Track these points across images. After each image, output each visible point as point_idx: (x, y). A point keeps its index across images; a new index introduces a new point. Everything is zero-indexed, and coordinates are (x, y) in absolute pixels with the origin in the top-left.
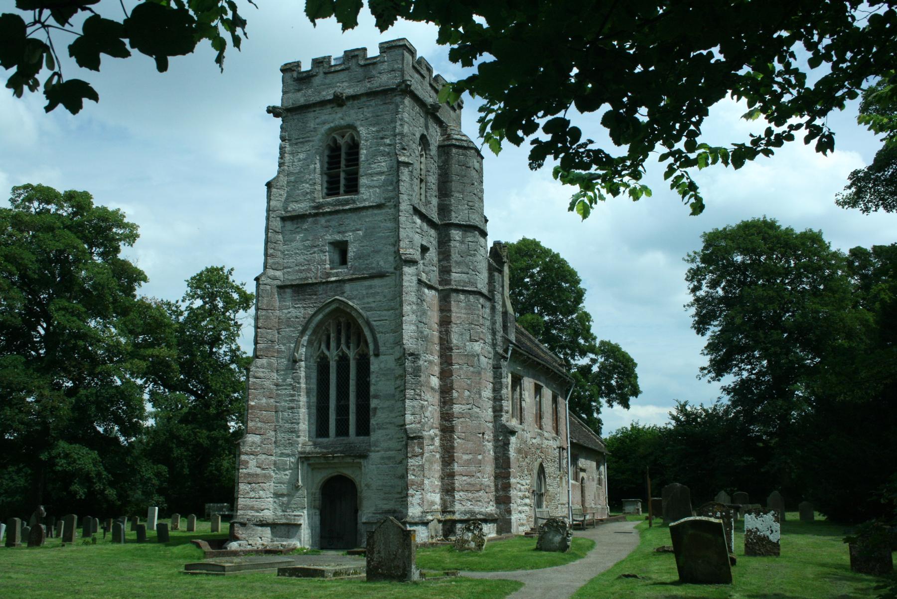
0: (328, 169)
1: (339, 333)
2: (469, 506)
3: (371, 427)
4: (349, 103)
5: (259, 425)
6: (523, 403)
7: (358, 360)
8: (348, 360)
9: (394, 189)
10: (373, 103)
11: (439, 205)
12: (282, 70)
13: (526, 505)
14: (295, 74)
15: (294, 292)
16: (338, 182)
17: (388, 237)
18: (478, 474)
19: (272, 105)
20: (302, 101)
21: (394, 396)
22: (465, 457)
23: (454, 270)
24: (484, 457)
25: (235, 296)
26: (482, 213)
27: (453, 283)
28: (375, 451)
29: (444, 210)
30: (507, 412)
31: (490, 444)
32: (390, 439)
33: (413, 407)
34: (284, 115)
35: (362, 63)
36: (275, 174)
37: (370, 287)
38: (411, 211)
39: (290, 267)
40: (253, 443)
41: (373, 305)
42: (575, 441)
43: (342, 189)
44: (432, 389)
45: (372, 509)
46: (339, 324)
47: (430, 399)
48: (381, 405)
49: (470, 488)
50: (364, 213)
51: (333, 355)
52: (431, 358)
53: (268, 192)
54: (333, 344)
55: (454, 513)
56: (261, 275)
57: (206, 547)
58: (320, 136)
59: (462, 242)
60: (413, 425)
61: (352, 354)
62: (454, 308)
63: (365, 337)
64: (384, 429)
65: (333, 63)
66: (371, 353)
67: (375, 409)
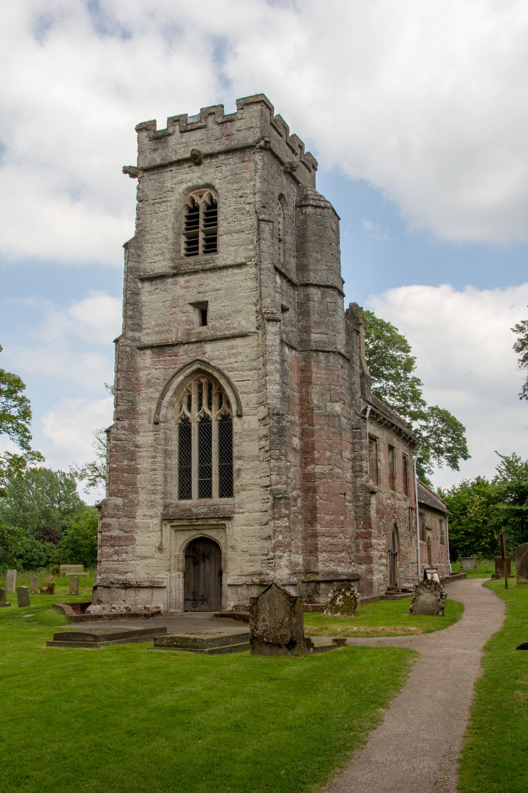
0: (187, 229)
1: (200, 395)
2: (332, 567)
3: (235, 488)
4: (206, 162)
6: (379, 463)
7: (220, 421)
8: (210, 422)
9: (255, 247)
11: (297, 265)
15: (154, 353)
16: (197, 242)
17: (249, 296)
18: (341, 535)
19: (128, 165)
20: (158, 162)
21: (258, 457)
22: (328, 518)
23: (313, 331)
24: (345, 518)
26: (340, 275)
27: (312, 343)
28: (239, 513)
29: (302, 268)
30: (367, 473)
31: (351, 504)
32: (256, 501)
34: (140, 175)
35: (220, 120)
36: (133, 235)
37: (232, 347)
38: (273, 270)
39: (149, 329)
40: (115, 505)
41: (235, 365)
42: (423, 502)
43: (201, 249)
44: (294, 449)
45: (238, 572)
46: (200, 386)
50: (224, 273)
51: (194, 417)
53: (125, 253)
54: (194, 406)
55: (317, 573)
56: (120, 337)
57: (70, 611)
58: (177, 196)
59: (321, 303)
60: (280, 486)
61: (214, 415)
62: (314, 370)
63: (227, 396)
65: (190, 121)
66: (234, 413)
67: (239, 470)
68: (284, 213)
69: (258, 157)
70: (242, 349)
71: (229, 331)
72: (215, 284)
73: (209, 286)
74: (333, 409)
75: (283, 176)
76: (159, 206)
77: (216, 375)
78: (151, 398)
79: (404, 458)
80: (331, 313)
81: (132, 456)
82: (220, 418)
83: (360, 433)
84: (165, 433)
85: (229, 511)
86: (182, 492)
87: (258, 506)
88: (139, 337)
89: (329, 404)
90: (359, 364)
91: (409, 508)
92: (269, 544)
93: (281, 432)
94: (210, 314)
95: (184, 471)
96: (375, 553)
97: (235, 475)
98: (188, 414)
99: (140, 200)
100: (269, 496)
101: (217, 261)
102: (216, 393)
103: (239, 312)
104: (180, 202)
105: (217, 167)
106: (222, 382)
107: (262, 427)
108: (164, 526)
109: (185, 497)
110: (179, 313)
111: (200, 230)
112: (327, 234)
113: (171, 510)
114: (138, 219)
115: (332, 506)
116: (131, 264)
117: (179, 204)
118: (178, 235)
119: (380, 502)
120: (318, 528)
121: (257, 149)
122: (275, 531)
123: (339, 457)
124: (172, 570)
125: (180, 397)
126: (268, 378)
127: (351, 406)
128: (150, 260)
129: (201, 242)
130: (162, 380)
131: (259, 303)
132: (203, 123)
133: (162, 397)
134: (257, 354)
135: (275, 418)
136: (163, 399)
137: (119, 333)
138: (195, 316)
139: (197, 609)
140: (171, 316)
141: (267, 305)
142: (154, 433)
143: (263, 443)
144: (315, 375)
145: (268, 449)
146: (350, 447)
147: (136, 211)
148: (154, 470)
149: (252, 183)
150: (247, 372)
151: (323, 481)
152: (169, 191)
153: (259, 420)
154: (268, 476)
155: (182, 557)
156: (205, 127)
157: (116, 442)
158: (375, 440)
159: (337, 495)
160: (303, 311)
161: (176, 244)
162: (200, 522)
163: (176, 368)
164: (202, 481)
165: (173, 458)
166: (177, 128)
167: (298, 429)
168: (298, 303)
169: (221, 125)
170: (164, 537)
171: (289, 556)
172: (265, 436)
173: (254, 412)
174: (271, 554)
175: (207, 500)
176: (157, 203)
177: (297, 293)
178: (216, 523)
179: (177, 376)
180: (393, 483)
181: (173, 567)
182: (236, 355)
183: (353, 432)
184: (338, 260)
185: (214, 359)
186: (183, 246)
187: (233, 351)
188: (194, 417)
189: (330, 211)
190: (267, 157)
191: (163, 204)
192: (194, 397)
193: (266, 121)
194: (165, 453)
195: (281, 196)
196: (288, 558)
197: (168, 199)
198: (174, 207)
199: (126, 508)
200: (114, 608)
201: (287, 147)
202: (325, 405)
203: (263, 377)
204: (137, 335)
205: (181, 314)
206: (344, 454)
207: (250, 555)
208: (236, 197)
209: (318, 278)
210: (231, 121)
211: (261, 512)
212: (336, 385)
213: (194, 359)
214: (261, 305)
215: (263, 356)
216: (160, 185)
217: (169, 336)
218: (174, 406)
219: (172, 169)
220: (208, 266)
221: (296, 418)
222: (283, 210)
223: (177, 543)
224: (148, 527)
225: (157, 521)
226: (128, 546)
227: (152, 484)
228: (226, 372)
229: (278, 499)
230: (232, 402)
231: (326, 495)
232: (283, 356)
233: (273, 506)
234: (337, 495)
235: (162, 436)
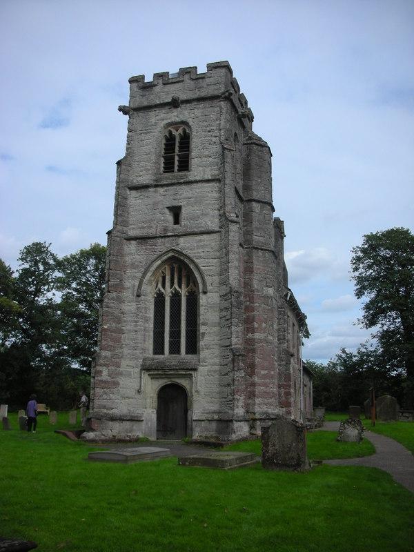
0: (165, 153)
2: (265, 409)
4: (183, 106)
5: (110, 343)
8: (181, 296)
12: (131, 81)
16: (173, 163)
18: (271, 386)
20: (146, 104)
22: (263, 372)
23: (255, 234)
25: (51, 262)
27: (254, 243)
32: (216, 357)
35: (194, 77)
40: (105, 357)
41: (202, 254)
43: (176, 168)
48: (208, 331)
50: (194, 186)
51: (168, 292)
54: (168, 284)
58: (159, 129)
66: (201, 291)
73: (183, 196)
98: (163, 290)
99: (130, 130)
103: (206, 215)
106: (192, 266)
113: (148, 363)
114: (129, 144)
120: (256, 379)
127: (278, 291)
129: (176, 163)
133: (144, 274)
137: (111, 227)
138: (170, 218)
139: (167, 437)
143: (224, 313)
147: (126, 139)
149: (218, 122)
153: (221, 296)
155: (155, 399)
156: (182, 81)
157: (107, 309)
161: (157, 163)
166: (161, 81)
173: (217, 290)
174: (231, 397)
182: (203, 247)
186: (163, 165)
188: (168, 292)
189: (267, 149)
190: (229, 106)
210: (203, 78)
215: (225, 248)
220: (182, 181)
223: (151, 387)
224: (131, 375)
225: (137, 370)
233: (233, 360)
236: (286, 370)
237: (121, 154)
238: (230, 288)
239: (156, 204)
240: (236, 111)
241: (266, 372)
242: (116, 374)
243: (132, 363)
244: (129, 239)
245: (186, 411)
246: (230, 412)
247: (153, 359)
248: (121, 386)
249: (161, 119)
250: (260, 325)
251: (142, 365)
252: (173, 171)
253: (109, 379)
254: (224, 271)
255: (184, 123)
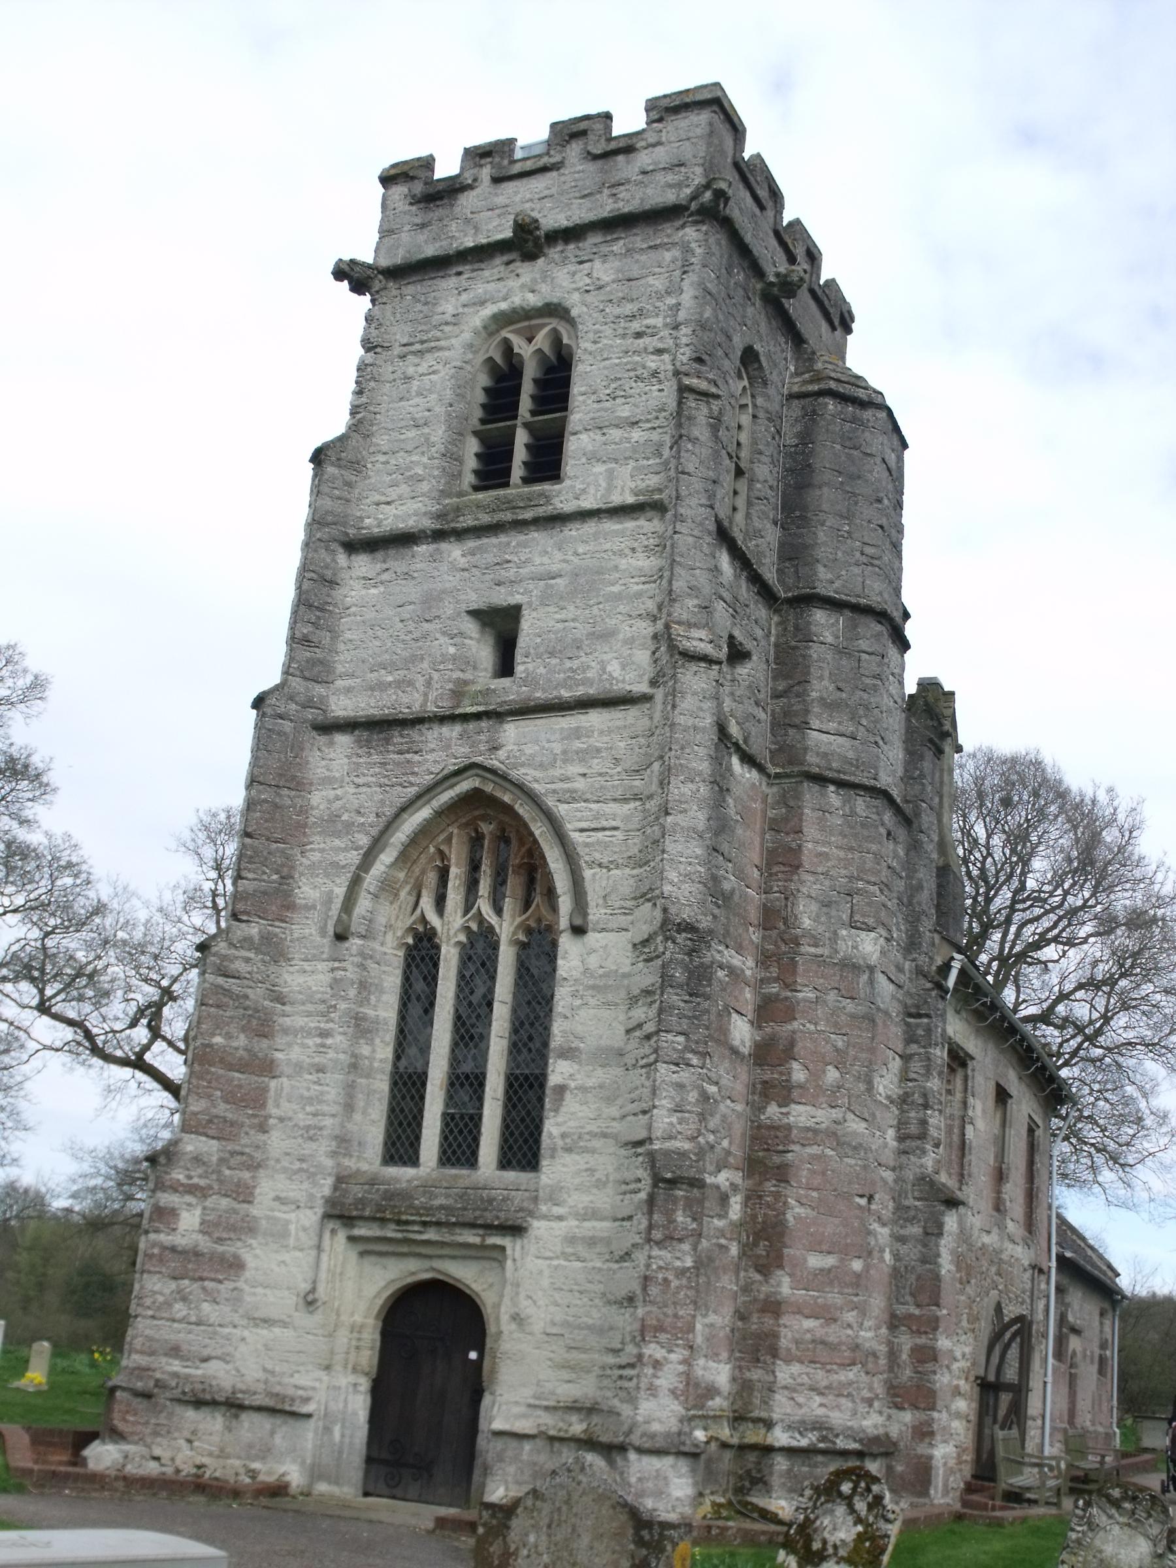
0: (483, 421)
1: (474, 867)
2: (815, 1407)
3: (545, 1141)
4: (554, 252)
5: (222, 1109)
6: (969, 1129)
8: (495, 946)
10: (618, 247)
11: (782, 545)
12: (387, 180)
13: (958, 1415)
14: (418, 188)
15: (358, 741)
17: (638, 595)
18: (850, 1317)
19: (346, 258)
20: (430, 251)
21: (621, 1054)
22: (815, 1261)
23: (815, 723)
24: (867, 1268)
27: (811, 758)
28: (545, 1217)
29: (794, 553)
32: (600, 1184)
33: (680, 1086)
34: (377, 285)
37: (577, 733)
39: (353, 676)
41: (580, 784)
42: (1068, 1254)
43: (517, 471)
44: (734, 1051)
45: (526, 1394)
46: (476, 841)
47: (726, 1080)
48: (580, 1079)
49: (816, 1352)
50: (573, 531)
51: (451, 928)
52: (736, 961)
53: (315, 476)
54: (455, 896)
58: (467, 336)
61: (506, 928)
62: (811, 831)
63: (548, 876)
64: (585, 1150)
66: (564, 923)
67: (561, 1089)
68: (755, 406)
69: (691, 233)
70: (606, 739)
71: (570, 688)
72: (546, 560)
74: (855, 947)
75: (758, 303)
76: (417, 360)
77: (523, 810)
78: (335, 865)
79: (1031, 1132)
80: (868, 681)
81: (262, 1026)
82: (522, 937)
83: (929, 1031)
84: (362, 967)
85: (521, 1210)
86: (394, 1144)
87: (605, 1200)
88: (323, 699)
89: (844, 932)
90: (936, 839)
91: (1033, 1267)
92: (625, 1321)
93: (698, 980)
94: (523, 642)
95: (405, 1084)
96: (943, 1380)
97: (548, 1103)
98: (434, 919)
99: (369, 345)
100: (640, 1173)
101: (556, 501)
102: (520, 866)
104: (475, 352)
105: (581, 263)
106: (539, 830)
107: (641, 965)
108: (327, 1235)
109: (401, 1158)
110: (438, 635)
111: (519, 421)
112: (871, 472)
113: (357, 1191)
114: (359, 392)
115: (829, 1230)
116: (327, 503)
117: (470, 356)
118: (460, 434)
119: (964, 1235)
120: (784, 1286)
121: (691, 215)
122: (646, 1280)
123: (862, 1087)
124: (339, 1368)
125: (417, 871)
126: (669, 819)
128: (378, 498)
129: (520, 454)
130: (372, 818)
131: (665, 611)
132: (557, 158)
134: (646, 754)
135: (680, 938)
136: (367, 871)
138: (484, 653)
139: (398, 1492)
140: (414, 645)
141: (684, 617)
142: (331, 964)
143: (639, 1013)
144: (810, 845)
145: (653, 1029)
146: (896, 1064)
147: (355, 374)
148: (318, 1071)
149: (671, 301)
150: (612, 805)
151: (809, 1150)
152: (447, 323)
154: (644, 1112)
155: (371, 1336)
157: (220, 980)
158: (964, 1065)
159: (848, 1197)
160: (790, 665)
161: (452, 456)
162: (431, 1235)
163: (412, 784)
164: (452, 1117)
165: (377, 1041)
166: (486, 173)
167: (748, 996)
168: (776, 645)
169: (600, 163)
170: (324, 1266)
171: (685, 1362)
172: (647, 992)
173: (623, 920)
174: (631, 1349)
175: (465, 1172)
176: (414, 353)
177: (776, 619)
178: (477, 1240)
179: (410, 811)
180: (999, 1192)
181: (339, 1358)
182: (584, 756)
183: (908, 1024)
184: (897, 548)
185: (523, 765)
186: (472, 463)
187: (578, 745)
188: (451, 928)
190: (718, 240)
191: (428, 356)
192: (456, 873)
193: (723, 152)
194: (357, 1026)
195: (749, 357)
196: (681, 1368)
197: (442, 343)
198: (458, 364)
199: (227, 1172)
200: (157, 1459)
201: (774, 242)
202: (835, 933)
203: (657, 818)
204: (319, 690)
205: (443, 640)
206: (877, 1080)
207: (570, 1348)
208: (624, 336)
209: (837, 584)
211: (615, 1220)
212: (868, 882)
213: (467, 762)
214: (669, 615)
216: (425, 308)
217: (405, 699)
218: (396, 895)
219: (460, 269)
220: (528, 515)
221: (747, 964)
222: (753, 396)
223: (362, 1288)
224: (285, 1234)
225: (311, 1217)
226: (220, 1282)
227: (308, 1109)
228: (550, 802)
229: (669, 1183)
230: (559, 891)
231: (815, 1194)
232: (723, 776)
233: (651, 1201)
234: (848, 1197)
235: (351, 973)
236: (924, 1260)
237: (334, 423)
238: (665, 910)
239: (430, 600)
240: (757, 271)
241: (830, 1261)
242: (233, 1228)
243: (296, 1190)
244: (329, 727)
245: (475, 1387)
246: (626, 1410)
247: (373, 1181)
248: (248, 1274)
249: (470, 307)
250: (816, 1076)
251: (330, 1202)
252: (506, 485)
253: (204, 1244)
254: (651, 852)
255: (556, 310)
